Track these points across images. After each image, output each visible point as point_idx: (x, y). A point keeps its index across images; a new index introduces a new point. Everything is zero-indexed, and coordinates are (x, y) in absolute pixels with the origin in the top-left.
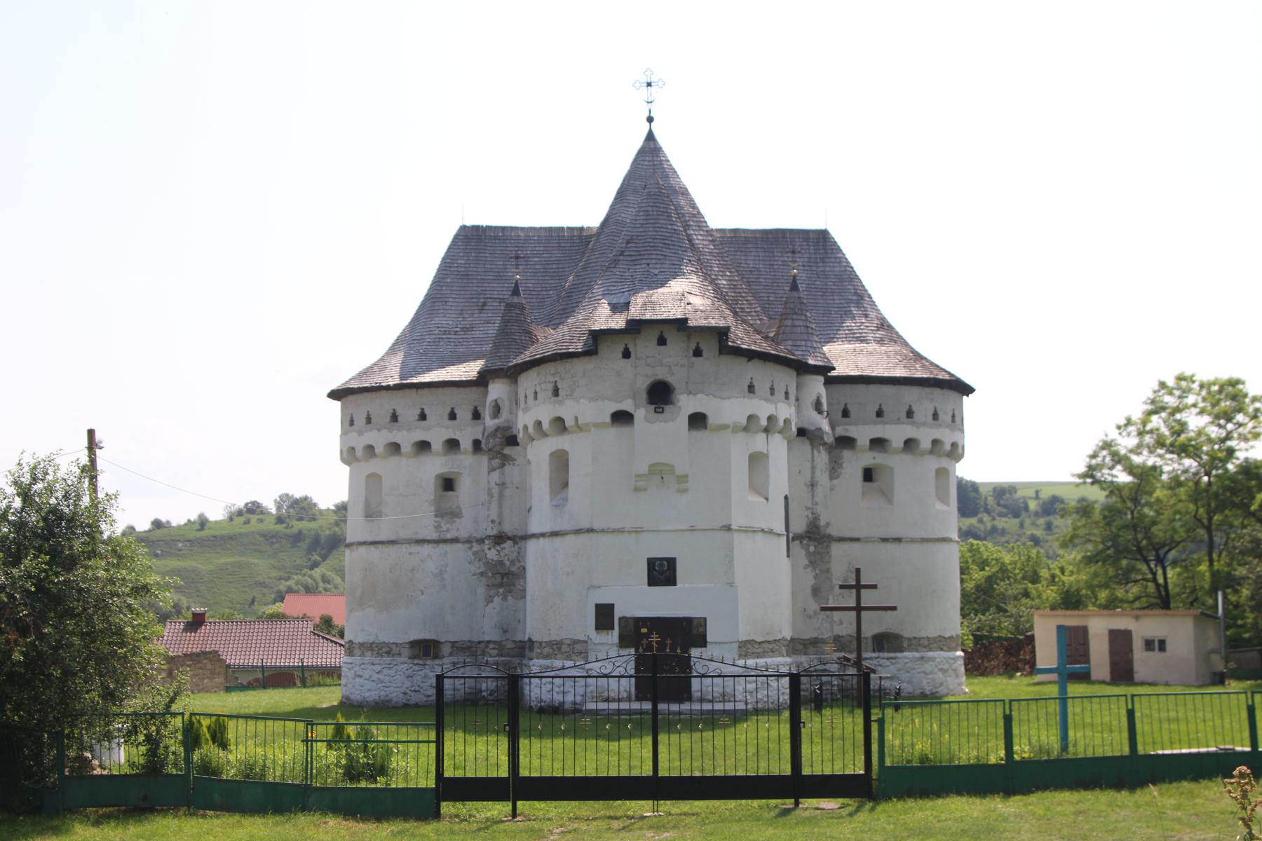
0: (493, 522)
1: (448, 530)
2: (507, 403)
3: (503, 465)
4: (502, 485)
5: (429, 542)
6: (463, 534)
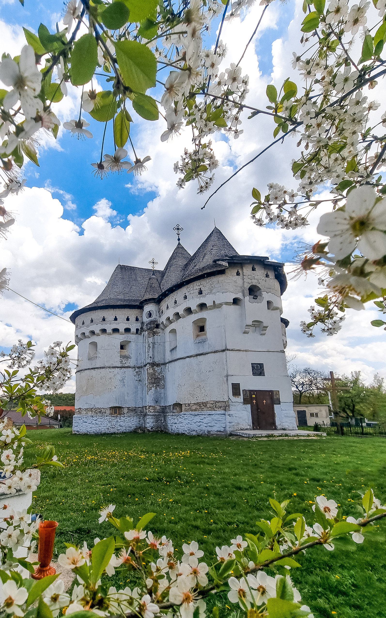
0: (151, 357)
1: (125, 363)
2: (155, 312)
3: (154, 335)
4: (154, 343)
5: (118, 367)
6: (132, 365)
